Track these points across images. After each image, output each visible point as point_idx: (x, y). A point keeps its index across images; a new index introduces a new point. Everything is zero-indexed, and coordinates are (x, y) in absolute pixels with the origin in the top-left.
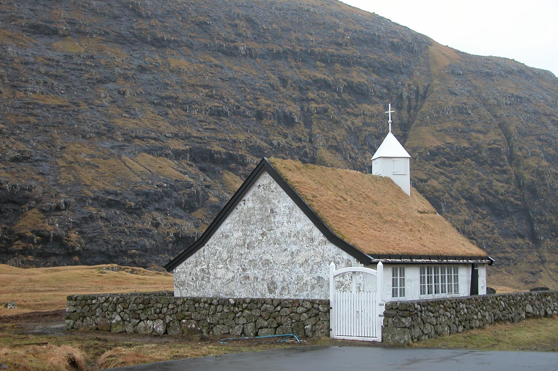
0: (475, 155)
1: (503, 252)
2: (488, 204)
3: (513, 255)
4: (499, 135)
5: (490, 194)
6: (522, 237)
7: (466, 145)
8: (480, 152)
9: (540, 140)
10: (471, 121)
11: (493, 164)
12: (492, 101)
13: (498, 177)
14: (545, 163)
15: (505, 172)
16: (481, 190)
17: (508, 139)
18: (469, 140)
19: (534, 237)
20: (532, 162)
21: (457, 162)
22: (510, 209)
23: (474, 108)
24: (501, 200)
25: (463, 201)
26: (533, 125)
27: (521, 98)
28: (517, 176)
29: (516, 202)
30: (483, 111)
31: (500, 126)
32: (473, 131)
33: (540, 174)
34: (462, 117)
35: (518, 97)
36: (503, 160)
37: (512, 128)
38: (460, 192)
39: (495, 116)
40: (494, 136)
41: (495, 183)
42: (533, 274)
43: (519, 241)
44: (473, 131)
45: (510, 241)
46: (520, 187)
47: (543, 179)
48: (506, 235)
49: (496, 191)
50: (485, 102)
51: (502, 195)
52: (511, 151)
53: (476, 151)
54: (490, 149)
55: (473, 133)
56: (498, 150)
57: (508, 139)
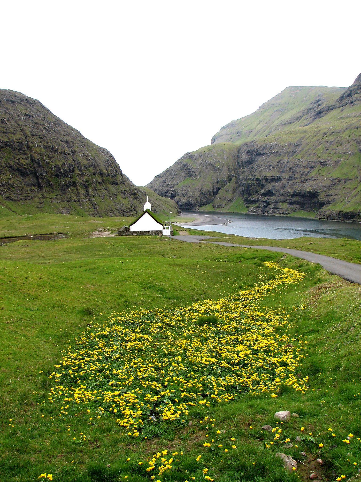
0: (11, 145)
1: (27, 193)
2: (18, 170)
3: (32, 195)
4: (21, 135)
5: (19, 165)
6: (34, 186)
7: (7, 140)
8: (13, 144)
9: (40, 138)
10: (8, 127)
11: (20, 150)
12: (17, 117)
13: (22, 157)
14: (43, 150)
15: (25, 154)
16: (15, 163)
17: (26, 137)
18: (8, 137)
19: (39, 186)
20: (38, 149)
21: (3, 149)
22: (29, 172)
23: (8, 120)
24: (24, 168)
25: (7, 169)
26: (36, 130)
27: (30, 116)
28: (31, 156)
29: (32, 169)
30: (13, 122)
31: (22, 130)
32: (9, 133)
33: (41, 155)
34: (3, 125)
35: (28, 115)
36: (24, 148)
37: (27, 132)
38: (6, 164)
39: (19, 125)
40: (19, 136)
41: (21, 160)
42: (41, 203)
43: (33, 188)
44: (9, 133)
45: (29, 188)
46: (32, 161)
47: (43, 158)
48: (27, 185)
49: (22, 164)
50: (13, 117)
51: (25, 165)
52: (28, 144)
53: (11, 143)
54: (18, 142)
55: (9, 134)
56: (22, 143)
57: (26, 137)
